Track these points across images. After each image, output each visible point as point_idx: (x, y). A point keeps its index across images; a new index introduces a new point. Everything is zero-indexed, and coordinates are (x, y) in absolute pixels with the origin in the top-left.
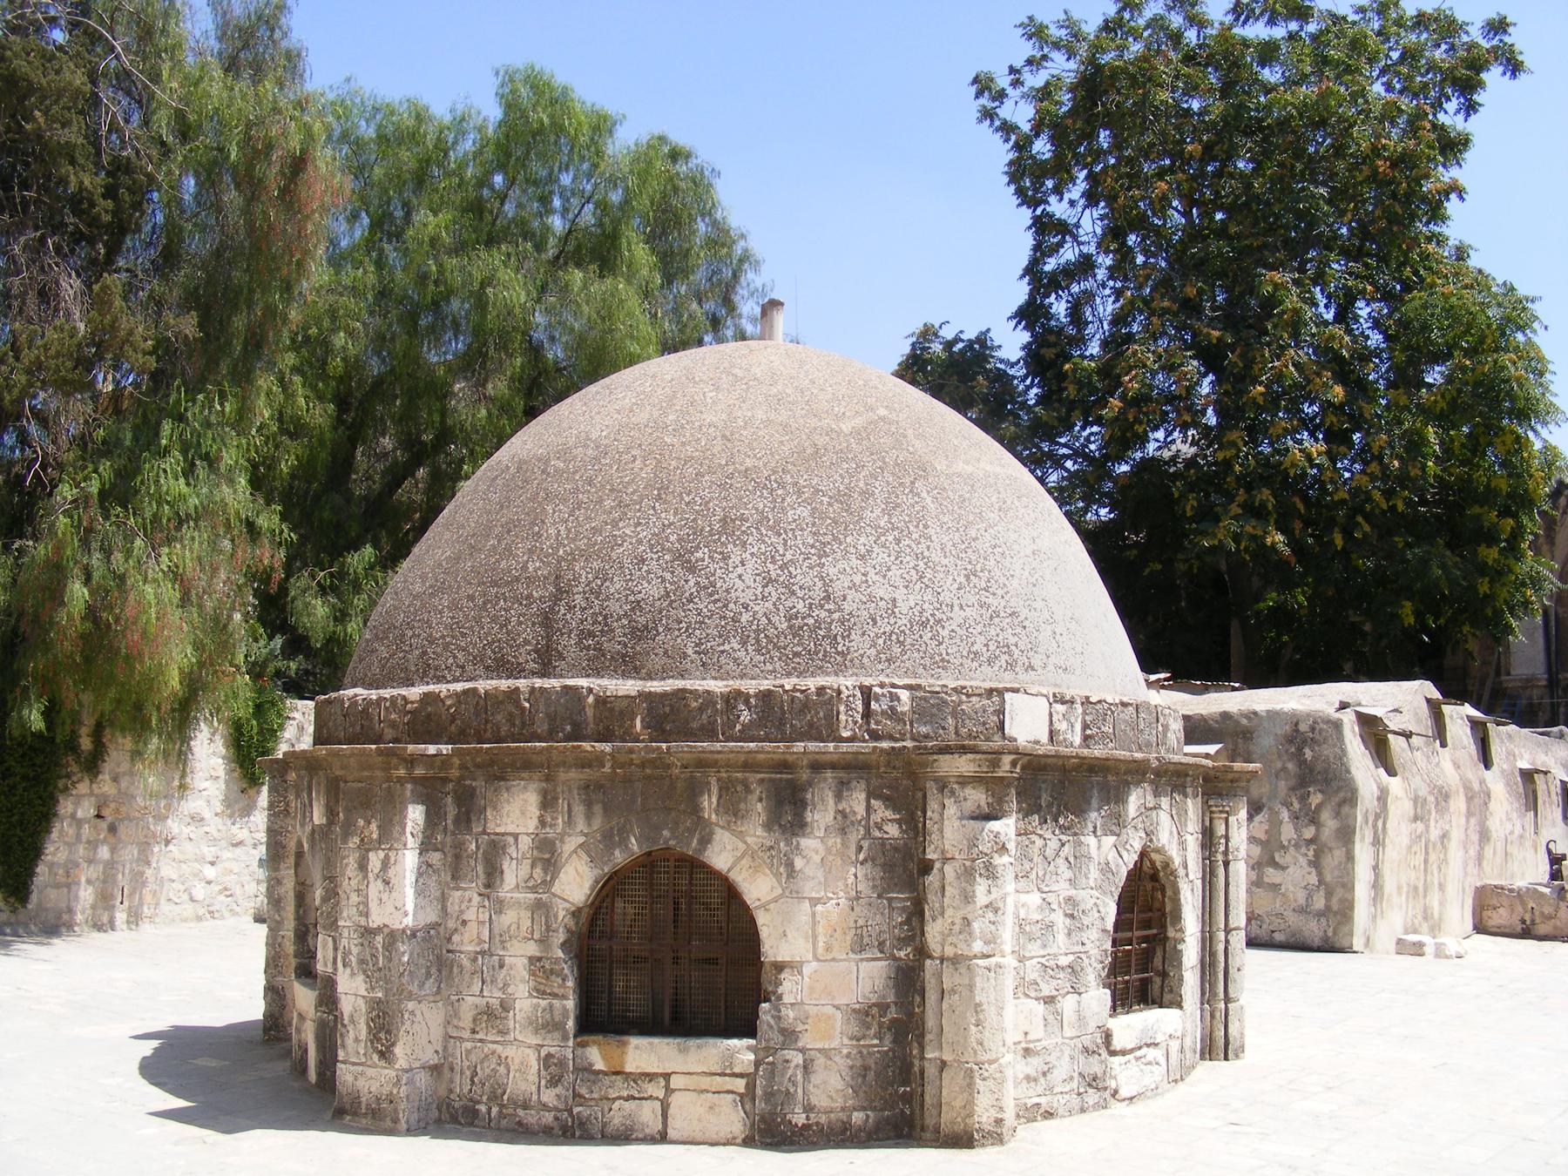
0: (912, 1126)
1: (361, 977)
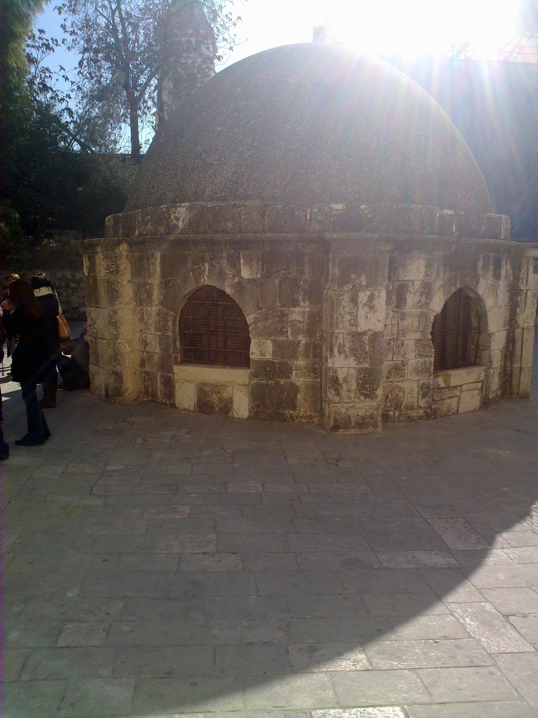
1: (353, 358)
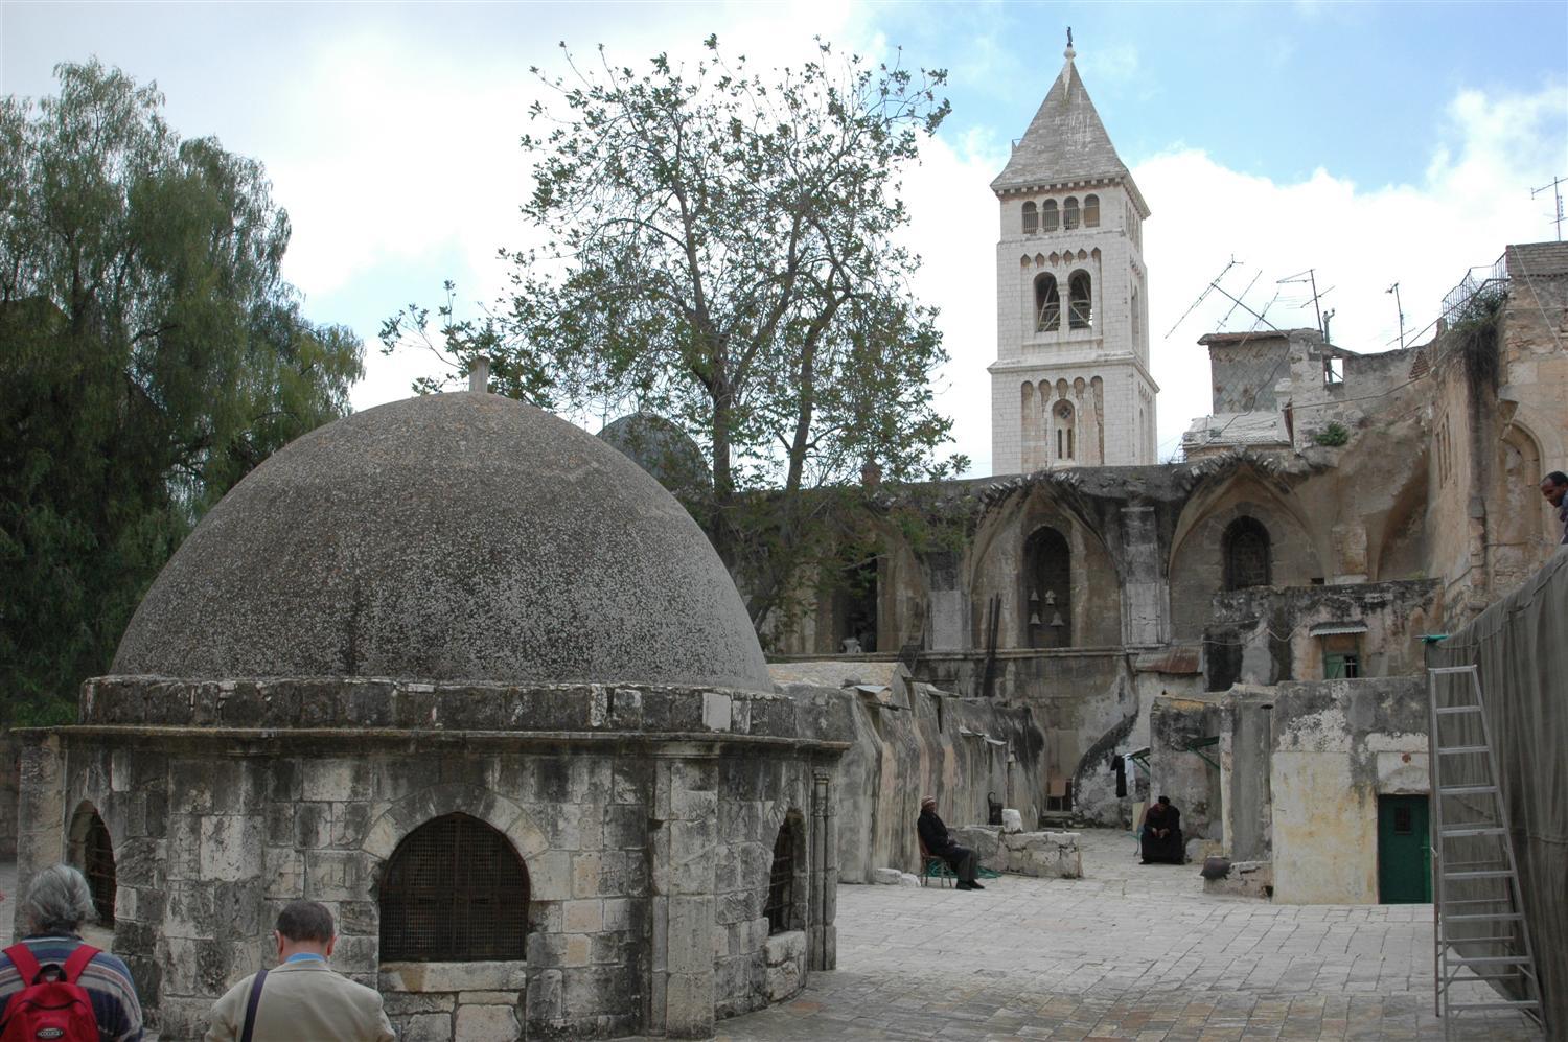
0: (641, 1025)
1: (192, 923)
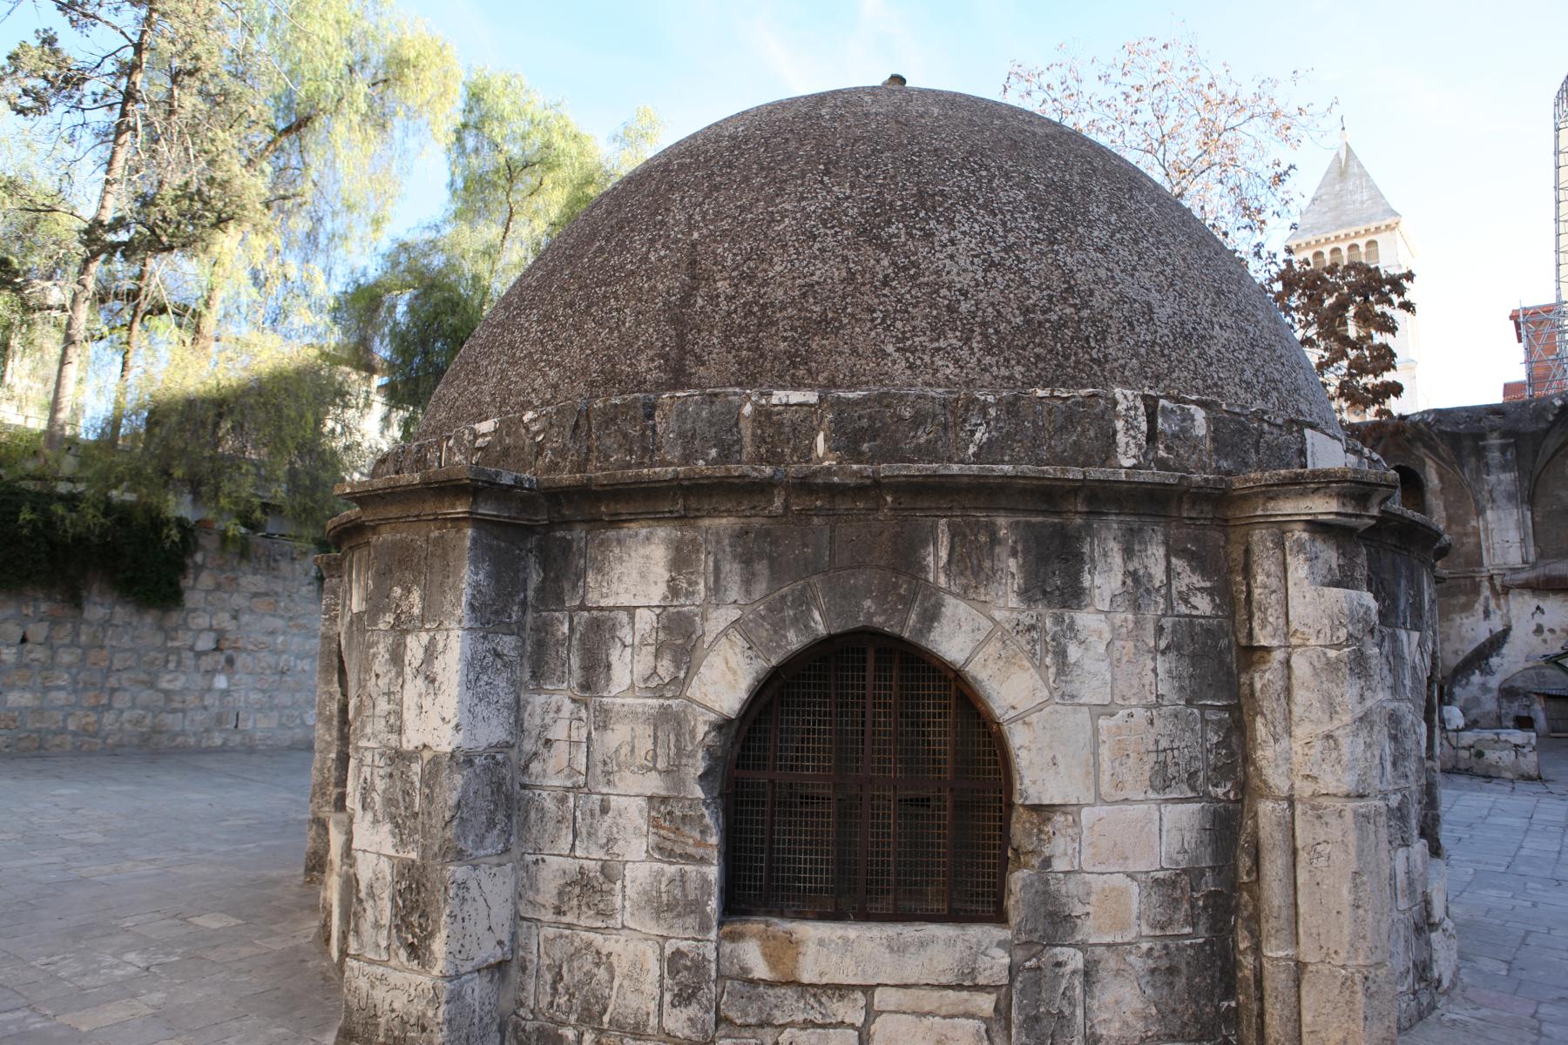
1: (388, 827)
